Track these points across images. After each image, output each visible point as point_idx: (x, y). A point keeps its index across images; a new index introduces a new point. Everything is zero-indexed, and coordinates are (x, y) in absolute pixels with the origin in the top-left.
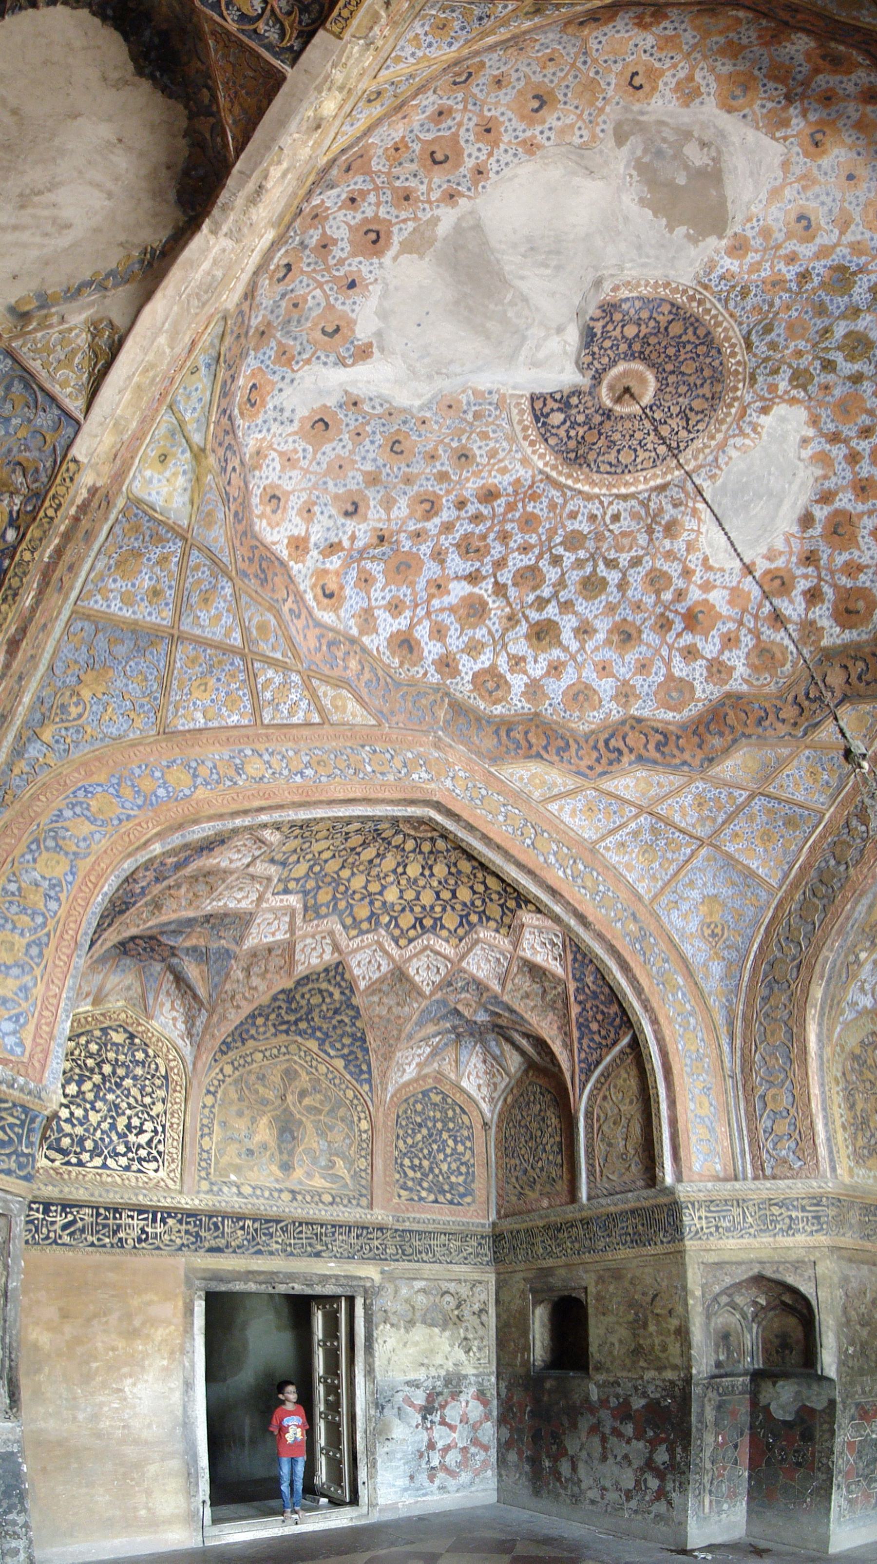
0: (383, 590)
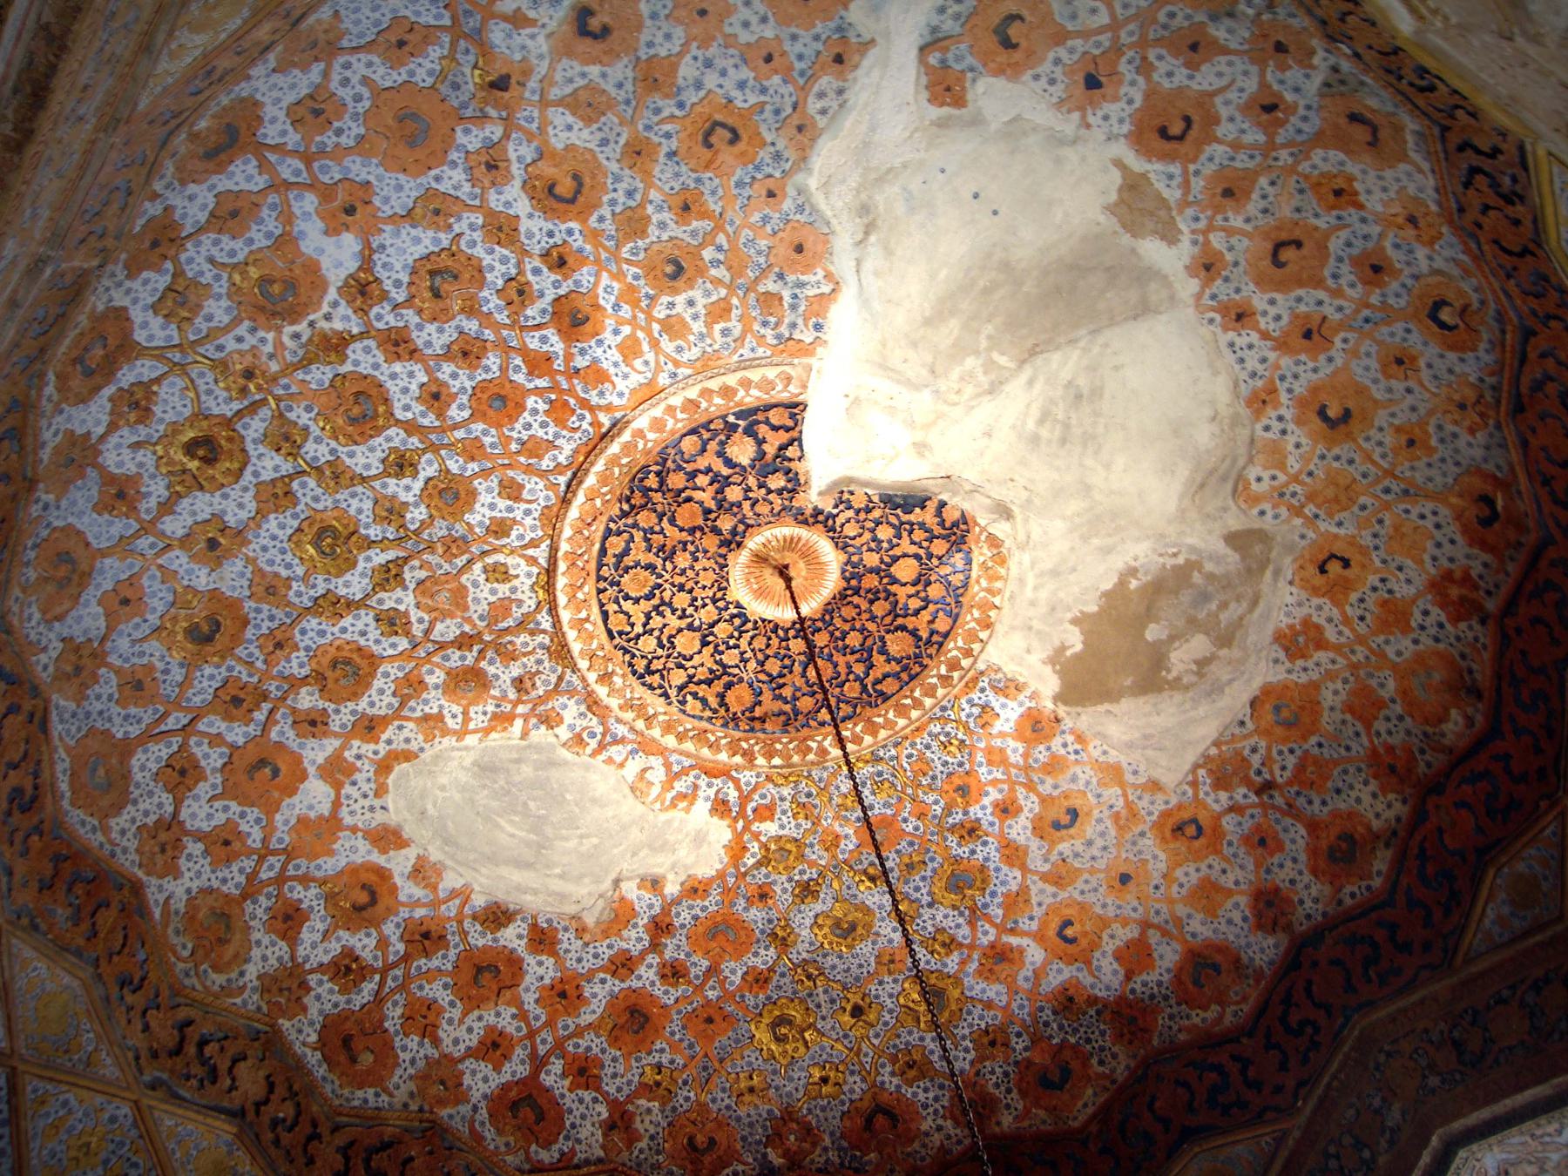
0: (365, 81)
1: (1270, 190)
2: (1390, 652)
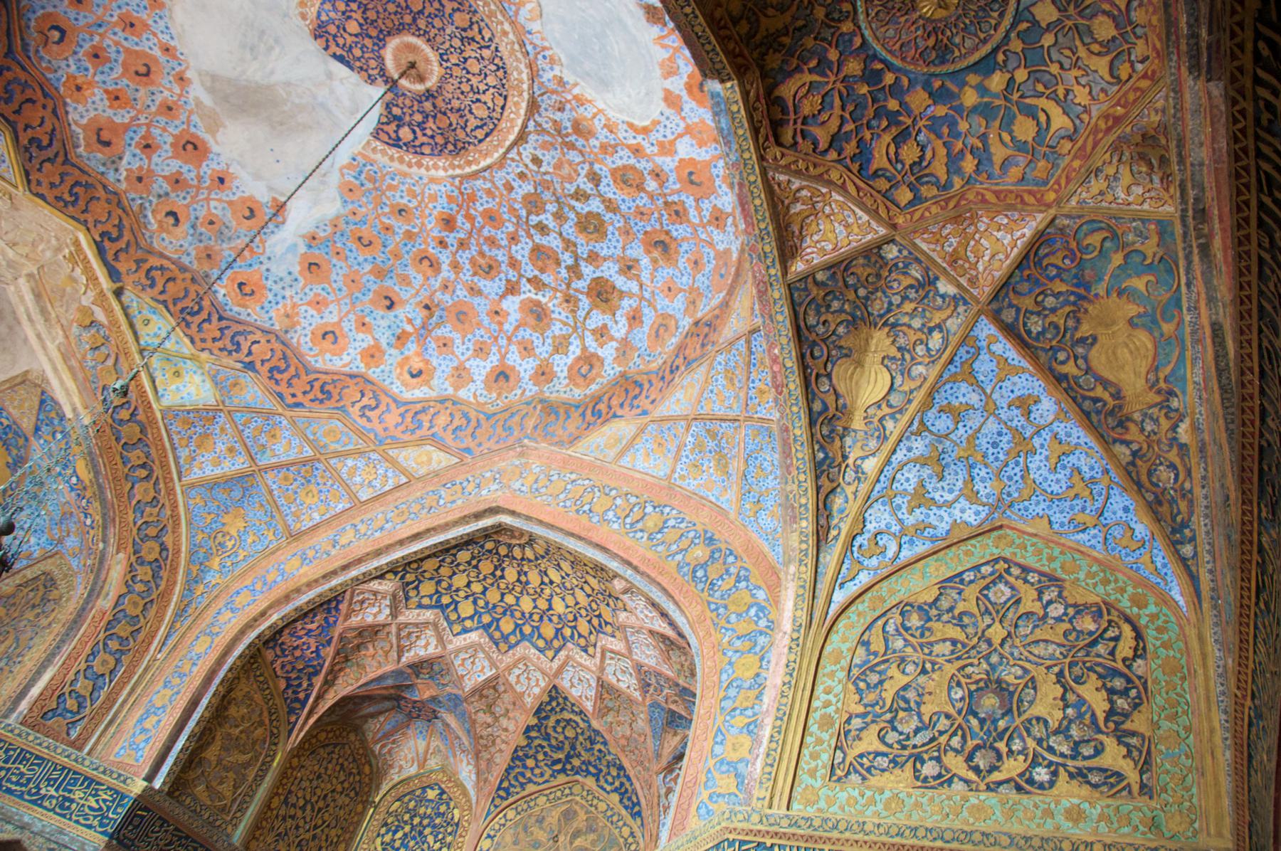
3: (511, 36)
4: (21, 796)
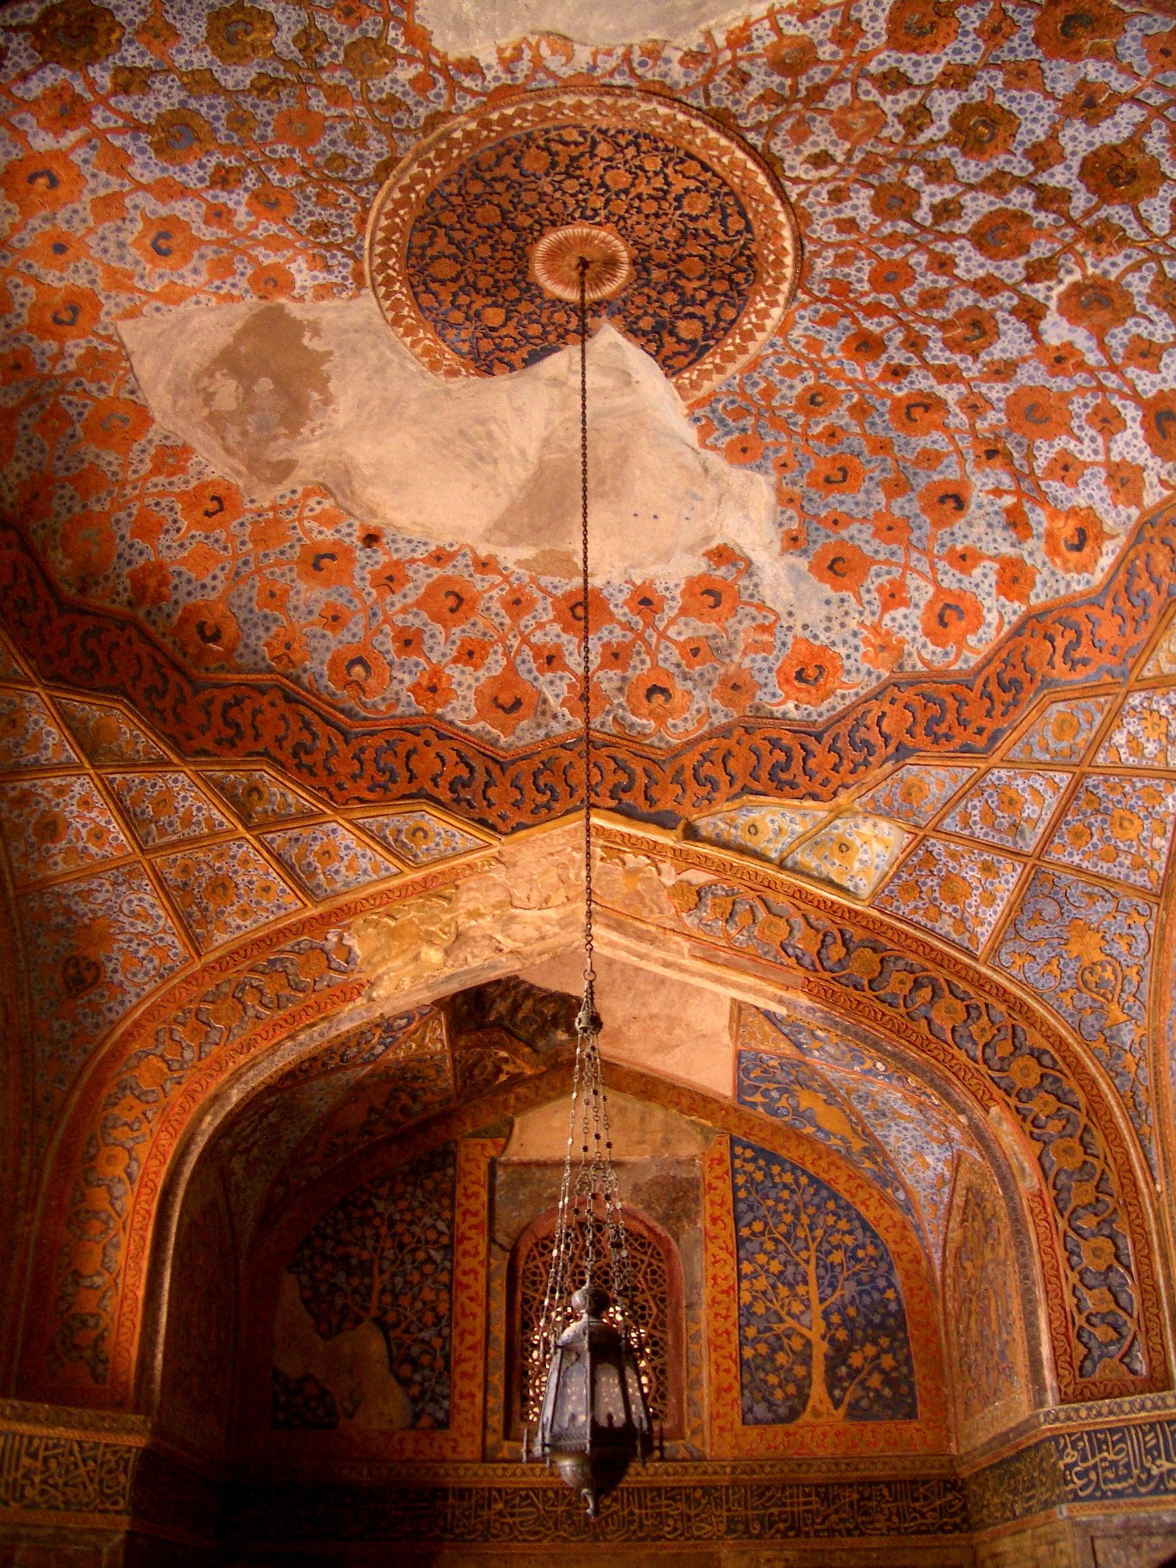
1: (497, 620)
2: (122, 515)
3: (587, 101)
4: (1137, 1494)
